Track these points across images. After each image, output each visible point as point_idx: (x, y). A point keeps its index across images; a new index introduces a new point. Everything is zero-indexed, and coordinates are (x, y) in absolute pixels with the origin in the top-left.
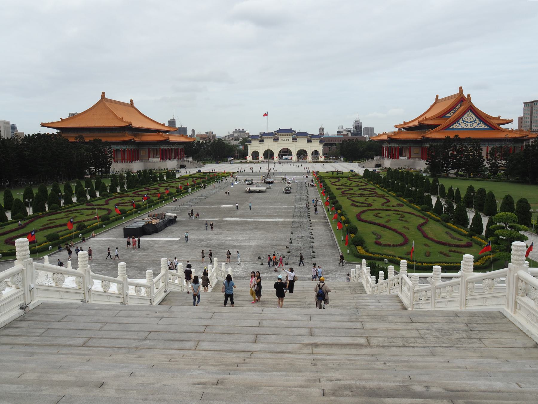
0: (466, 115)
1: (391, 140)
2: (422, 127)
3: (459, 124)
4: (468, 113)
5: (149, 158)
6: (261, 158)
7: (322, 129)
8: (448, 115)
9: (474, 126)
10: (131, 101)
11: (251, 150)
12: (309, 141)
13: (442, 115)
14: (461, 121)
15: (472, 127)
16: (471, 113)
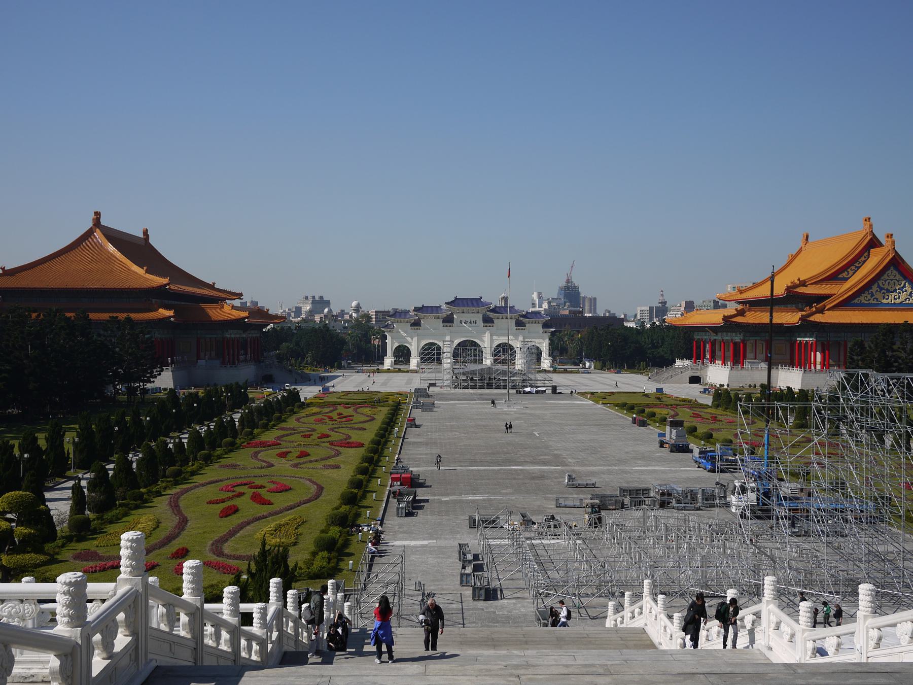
0: (885, 276)
1: (729, 324)
2: (794, 298)
3: (872, 295)
4: (889, 272)
5: (199, 358)
6: (414, 362)
7: (506, 299)
8: (845, 275)
9: (901, 300)
10: (146, 233)
11: (391, 344)
12: (519, 324)
13: (835, 276)
14: (875, 288)
15: (898, 301)
16: (894, 272)
